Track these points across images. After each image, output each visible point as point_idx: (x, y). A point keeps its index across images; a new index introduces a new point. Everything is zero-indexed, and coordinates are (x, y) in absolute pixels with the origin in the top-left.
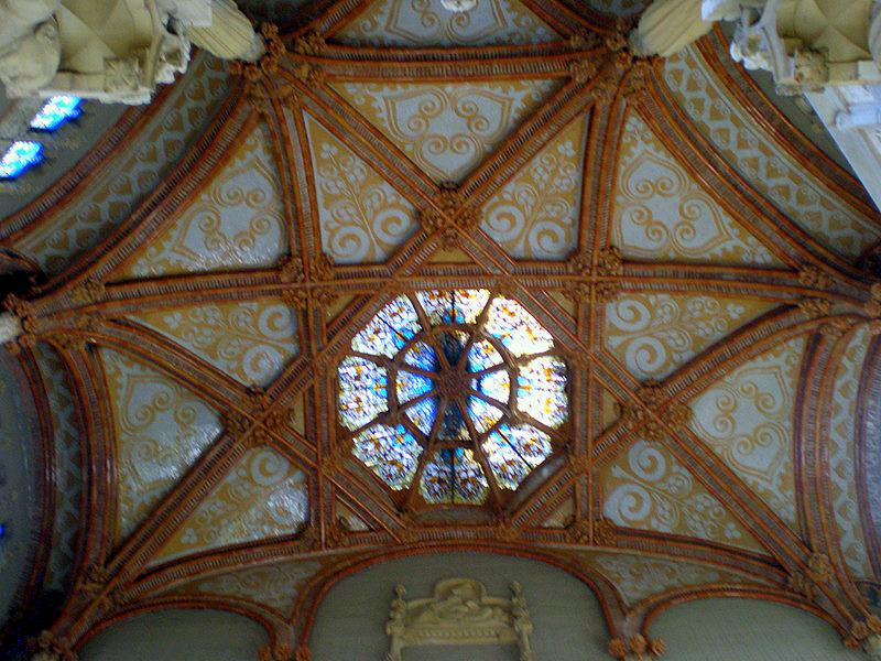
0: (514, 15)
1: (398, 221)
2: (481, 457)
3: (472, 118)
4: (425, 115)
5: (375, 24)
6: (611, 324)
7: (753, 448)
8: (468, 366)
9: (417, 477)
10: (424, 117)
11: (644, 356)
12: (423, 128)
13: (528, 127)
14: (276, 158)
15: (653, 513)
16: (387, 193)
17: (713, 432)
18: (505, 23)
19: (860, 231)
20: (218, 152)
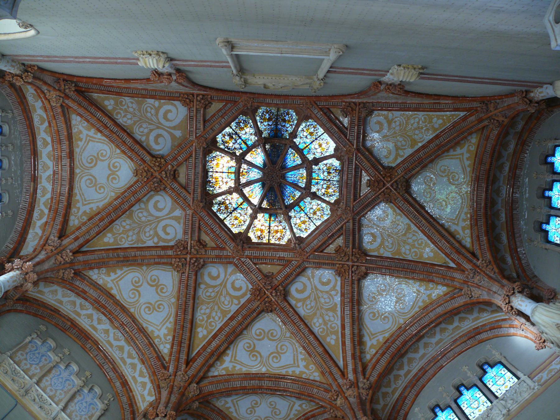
0: (227, 406)
1: (297, 290)
2: (258, 132)
3: (252, 351)
4: (277, 354)
5: (300, 406)
6: (179, 223)
7: (98, 154)
8: (263, 186)
9: (298, 125)
10: (278, 353)
11: (160, 205)
12: (279, 346)
13: (222, 349)
14: (361, 336)
15: (157, 110)
16: (301, 308)
17: (121, 161)
18: (232, 401)
19: (41, 291)
20: (392, 349)
